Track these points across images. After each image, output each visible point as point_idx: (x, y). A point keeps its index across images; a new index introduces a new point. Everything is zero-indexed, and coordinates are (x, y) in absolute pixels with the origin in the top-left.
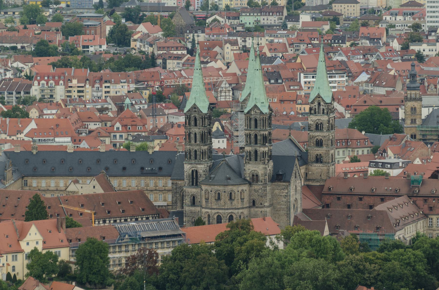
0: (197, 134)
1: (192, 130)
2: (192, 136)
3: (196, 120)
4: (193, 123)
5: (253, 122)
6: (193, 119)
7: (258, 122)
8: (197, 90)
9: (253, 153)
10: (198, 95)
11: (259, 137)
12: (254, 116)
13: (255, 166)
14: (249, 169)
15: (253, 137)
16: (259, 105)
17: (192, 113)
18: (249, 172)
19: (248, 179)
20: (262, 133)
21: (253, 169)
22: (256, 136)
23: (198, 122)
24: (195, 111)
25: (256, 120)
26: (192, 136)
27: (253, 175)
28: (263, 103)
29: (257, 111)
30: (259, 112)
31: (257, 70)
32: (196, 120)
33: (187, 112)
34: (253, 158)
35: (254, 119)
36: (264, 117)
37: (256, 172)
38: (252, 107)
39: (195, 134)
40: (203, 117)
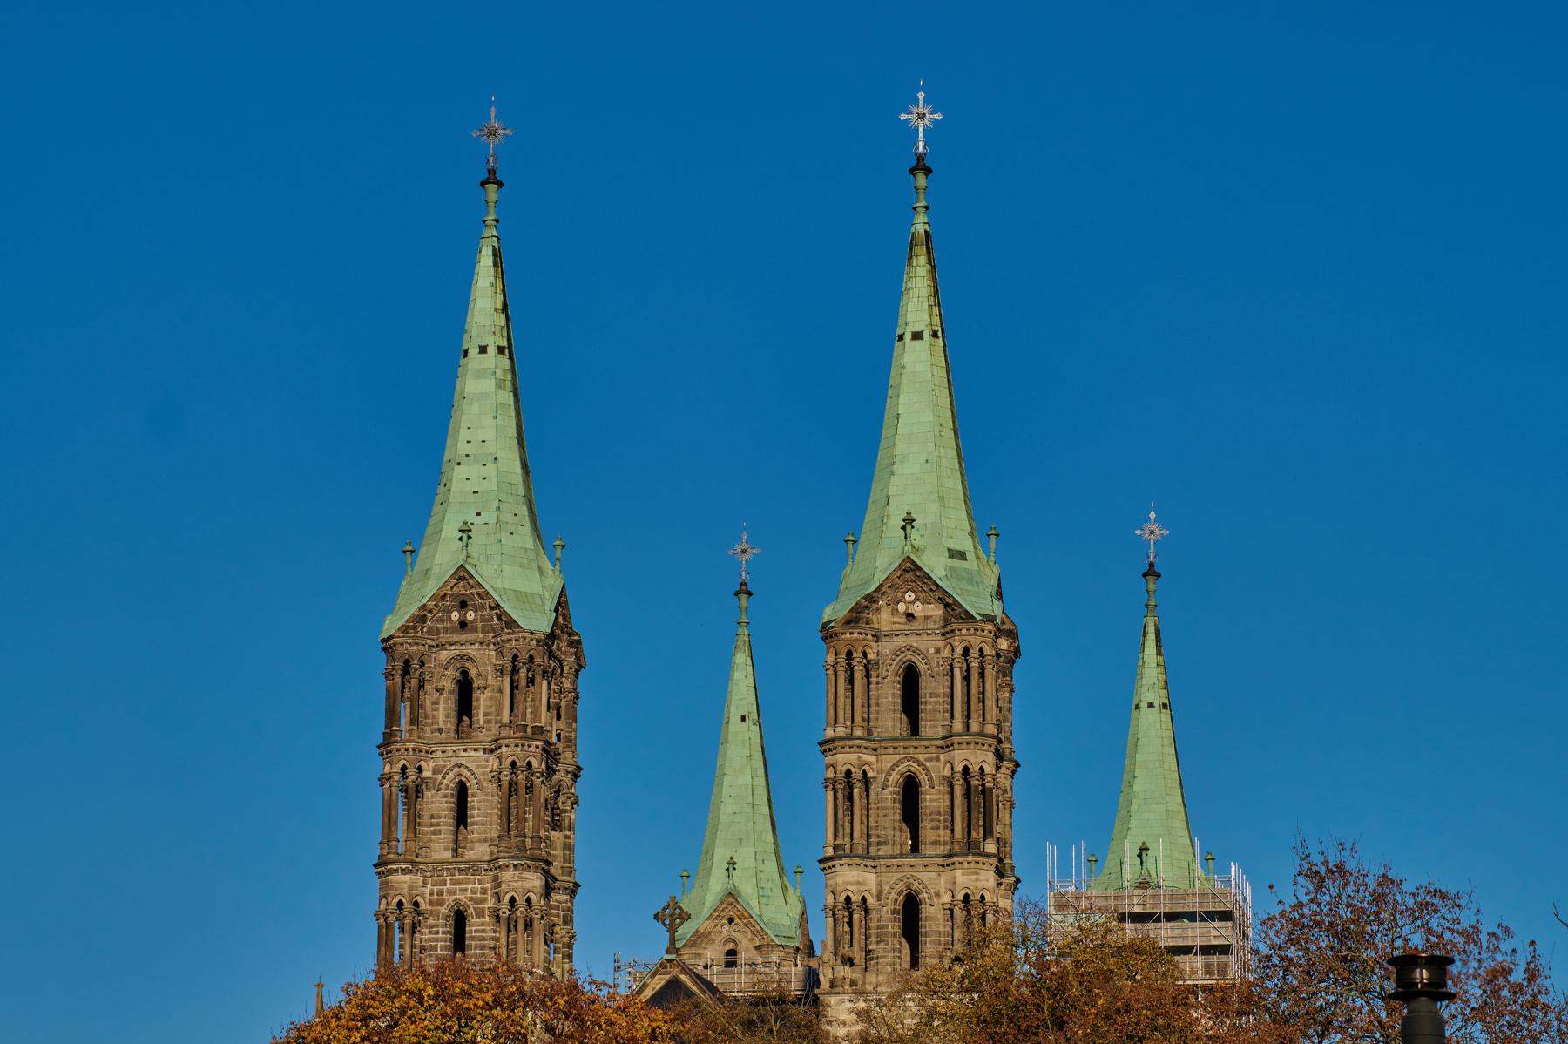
0: (472, 789)
1: (439, 759)
2: (438, 804)
3: (465, 691)
4: (442, 709)
5: (889, 692)
6: (449, 684)
7: (926, 686)
8: (481, 486)
9: (886, 916)
10: (489, 516)
11: (932, 799)
12: (899, 642)
15: (887, 795)
16: (936, 565)
17: (444, 638)
20: (961, 757)
22: (910, 790)
23: (482, 702)
24: (463, 625)
25: (910, 678)
26: (438, 804)
28: (960, 555)
29: (918, 609)
30: (936, 611)
31: (917, 336)
32: (465, 691)
33: (405, 629)
38: (880, 577)
39: (462, 791)
40: (523, 659)
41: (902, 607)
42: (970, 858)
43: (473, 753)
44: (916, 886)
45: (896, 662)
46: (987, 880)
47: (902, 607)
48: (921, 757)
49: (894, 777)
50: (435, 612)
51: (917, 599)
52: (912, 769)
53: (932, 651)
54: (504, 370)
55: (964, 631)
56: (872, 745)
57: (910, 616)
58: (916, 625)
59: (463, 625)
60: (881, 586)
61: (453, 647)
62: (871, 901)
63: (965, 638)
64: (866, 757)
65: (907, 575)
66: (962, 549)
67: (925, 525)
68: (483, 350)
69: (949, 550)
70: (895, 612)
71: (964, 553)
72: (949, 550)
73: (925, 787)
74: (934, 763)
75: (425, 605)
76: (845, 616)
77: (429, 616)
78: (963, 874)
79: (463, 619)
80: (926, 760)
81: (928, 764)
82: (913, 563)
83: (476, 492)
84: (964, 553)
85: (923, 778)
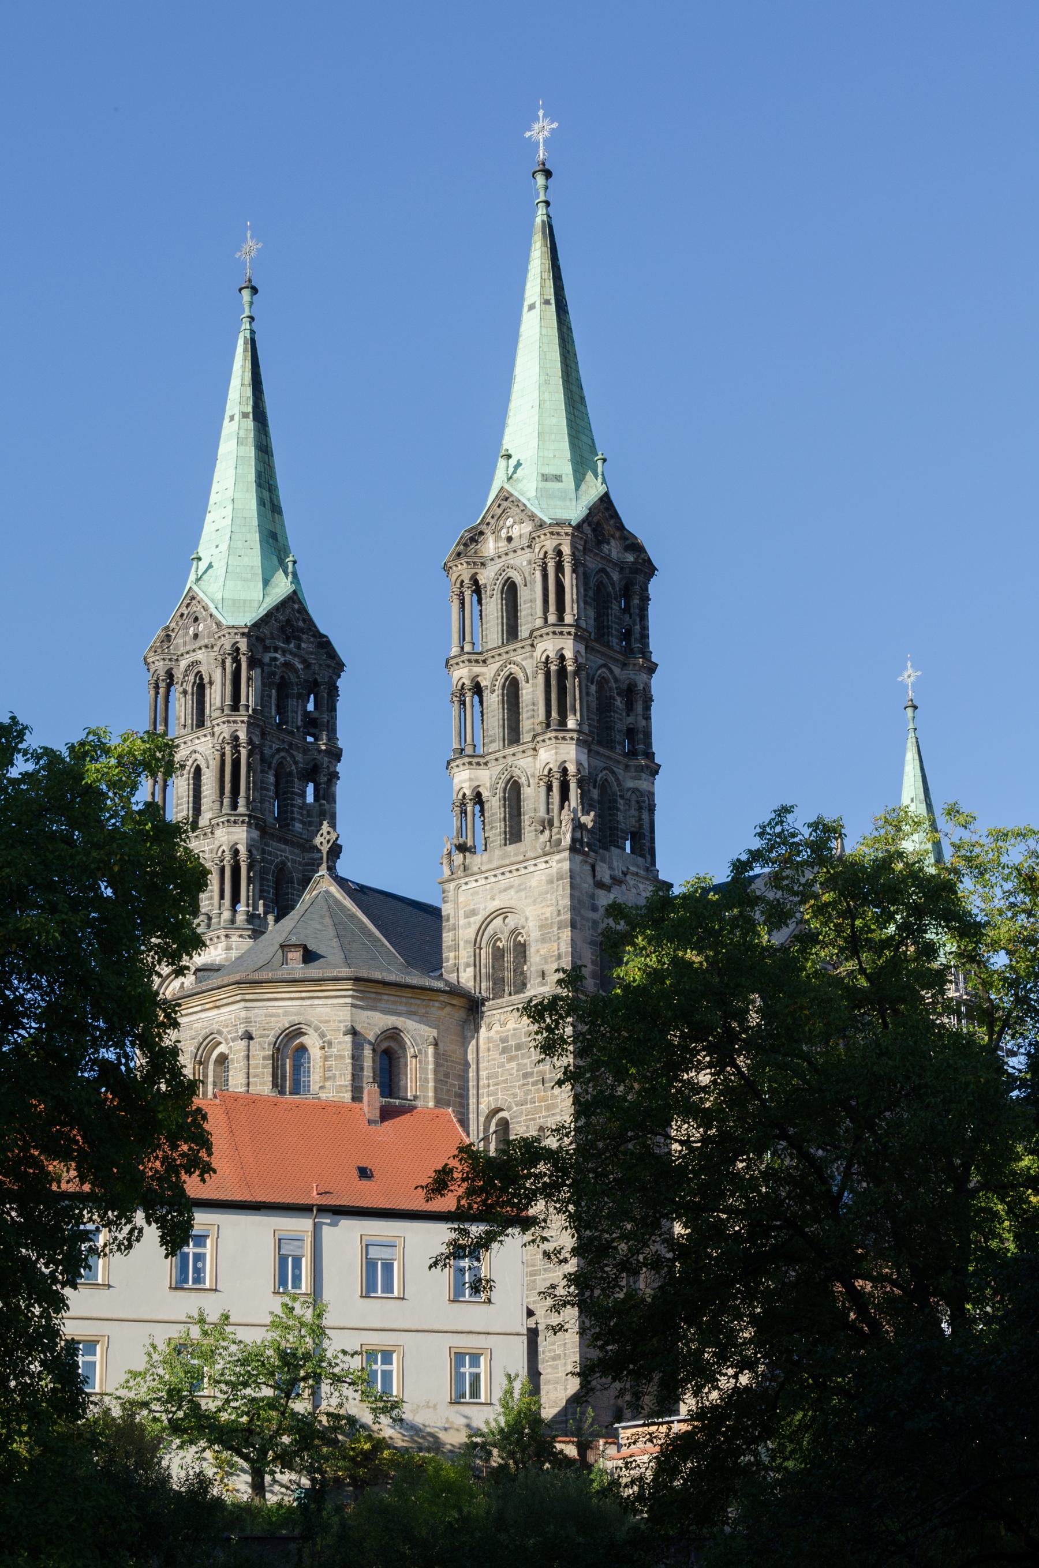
9: (495, 805)
12: (498, 564)
13: (504, 881)
14: (473, 913)
15: (493, 700)
18: (469, 933)
19: (466, 978)
21: (497, 904)
25: (510, 591)
27: (498, 954)
28: (558, 478)
29: (515, 532)
34: (496, 830)
35: (498, 587)
36: (550, 544)
37: (512, 921)
41: (504, 533)
42: (549, 735)
43: (203, 739)
44: (517, 772)
45: (498, 582)
46: (568, 753)
47: (504, 533)
48: (518, 659)
49: (499, 683)
50: (176, 631)
51: (515, 523)
52: (513, 671)
53: (525, 563)
54: (247, 430)
55: (542, 536)
56: (481, 658)
57: (510, 539)
58: (513, 544)
59: (196, 636)
60: (484, 517)
61: (188, 656)
62: (485, 794)
63: (543, 544)
64: (477, 669)
65: (505, 504)
66: (558, 473)
67: (526, 459)
68: (232, 418)
69: (543, 475)
70: (498, 539)
71: (560, 476)
72: (543, 475)
73: (522, 683)
74: (529, 661)
75: (168, 627)
76: (454, 551)
77: (173, 635)
78: (546, 752)
79: (196, 631)
80: (523, 660)
81: (524, 663)
82: (508, 492)
83: (218, 530)
84: (560, 476)
85: (521, 677)
